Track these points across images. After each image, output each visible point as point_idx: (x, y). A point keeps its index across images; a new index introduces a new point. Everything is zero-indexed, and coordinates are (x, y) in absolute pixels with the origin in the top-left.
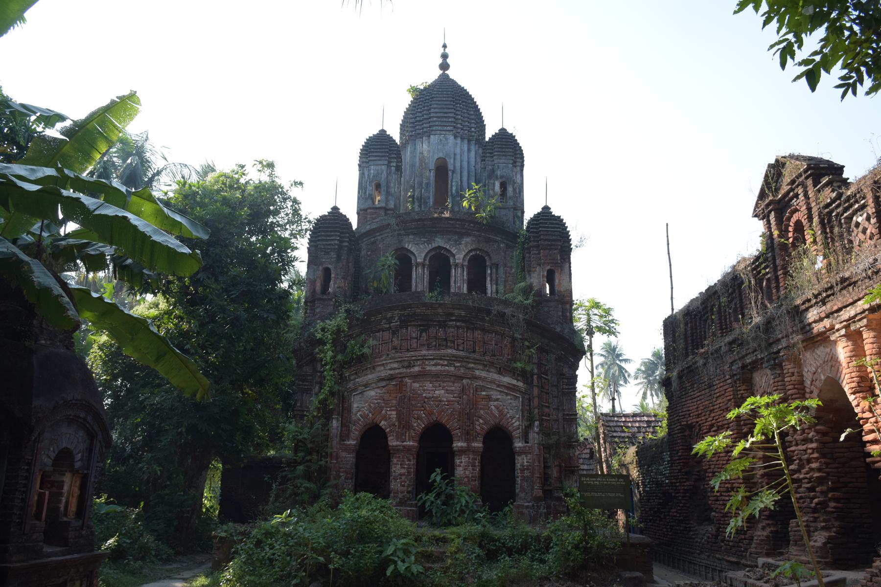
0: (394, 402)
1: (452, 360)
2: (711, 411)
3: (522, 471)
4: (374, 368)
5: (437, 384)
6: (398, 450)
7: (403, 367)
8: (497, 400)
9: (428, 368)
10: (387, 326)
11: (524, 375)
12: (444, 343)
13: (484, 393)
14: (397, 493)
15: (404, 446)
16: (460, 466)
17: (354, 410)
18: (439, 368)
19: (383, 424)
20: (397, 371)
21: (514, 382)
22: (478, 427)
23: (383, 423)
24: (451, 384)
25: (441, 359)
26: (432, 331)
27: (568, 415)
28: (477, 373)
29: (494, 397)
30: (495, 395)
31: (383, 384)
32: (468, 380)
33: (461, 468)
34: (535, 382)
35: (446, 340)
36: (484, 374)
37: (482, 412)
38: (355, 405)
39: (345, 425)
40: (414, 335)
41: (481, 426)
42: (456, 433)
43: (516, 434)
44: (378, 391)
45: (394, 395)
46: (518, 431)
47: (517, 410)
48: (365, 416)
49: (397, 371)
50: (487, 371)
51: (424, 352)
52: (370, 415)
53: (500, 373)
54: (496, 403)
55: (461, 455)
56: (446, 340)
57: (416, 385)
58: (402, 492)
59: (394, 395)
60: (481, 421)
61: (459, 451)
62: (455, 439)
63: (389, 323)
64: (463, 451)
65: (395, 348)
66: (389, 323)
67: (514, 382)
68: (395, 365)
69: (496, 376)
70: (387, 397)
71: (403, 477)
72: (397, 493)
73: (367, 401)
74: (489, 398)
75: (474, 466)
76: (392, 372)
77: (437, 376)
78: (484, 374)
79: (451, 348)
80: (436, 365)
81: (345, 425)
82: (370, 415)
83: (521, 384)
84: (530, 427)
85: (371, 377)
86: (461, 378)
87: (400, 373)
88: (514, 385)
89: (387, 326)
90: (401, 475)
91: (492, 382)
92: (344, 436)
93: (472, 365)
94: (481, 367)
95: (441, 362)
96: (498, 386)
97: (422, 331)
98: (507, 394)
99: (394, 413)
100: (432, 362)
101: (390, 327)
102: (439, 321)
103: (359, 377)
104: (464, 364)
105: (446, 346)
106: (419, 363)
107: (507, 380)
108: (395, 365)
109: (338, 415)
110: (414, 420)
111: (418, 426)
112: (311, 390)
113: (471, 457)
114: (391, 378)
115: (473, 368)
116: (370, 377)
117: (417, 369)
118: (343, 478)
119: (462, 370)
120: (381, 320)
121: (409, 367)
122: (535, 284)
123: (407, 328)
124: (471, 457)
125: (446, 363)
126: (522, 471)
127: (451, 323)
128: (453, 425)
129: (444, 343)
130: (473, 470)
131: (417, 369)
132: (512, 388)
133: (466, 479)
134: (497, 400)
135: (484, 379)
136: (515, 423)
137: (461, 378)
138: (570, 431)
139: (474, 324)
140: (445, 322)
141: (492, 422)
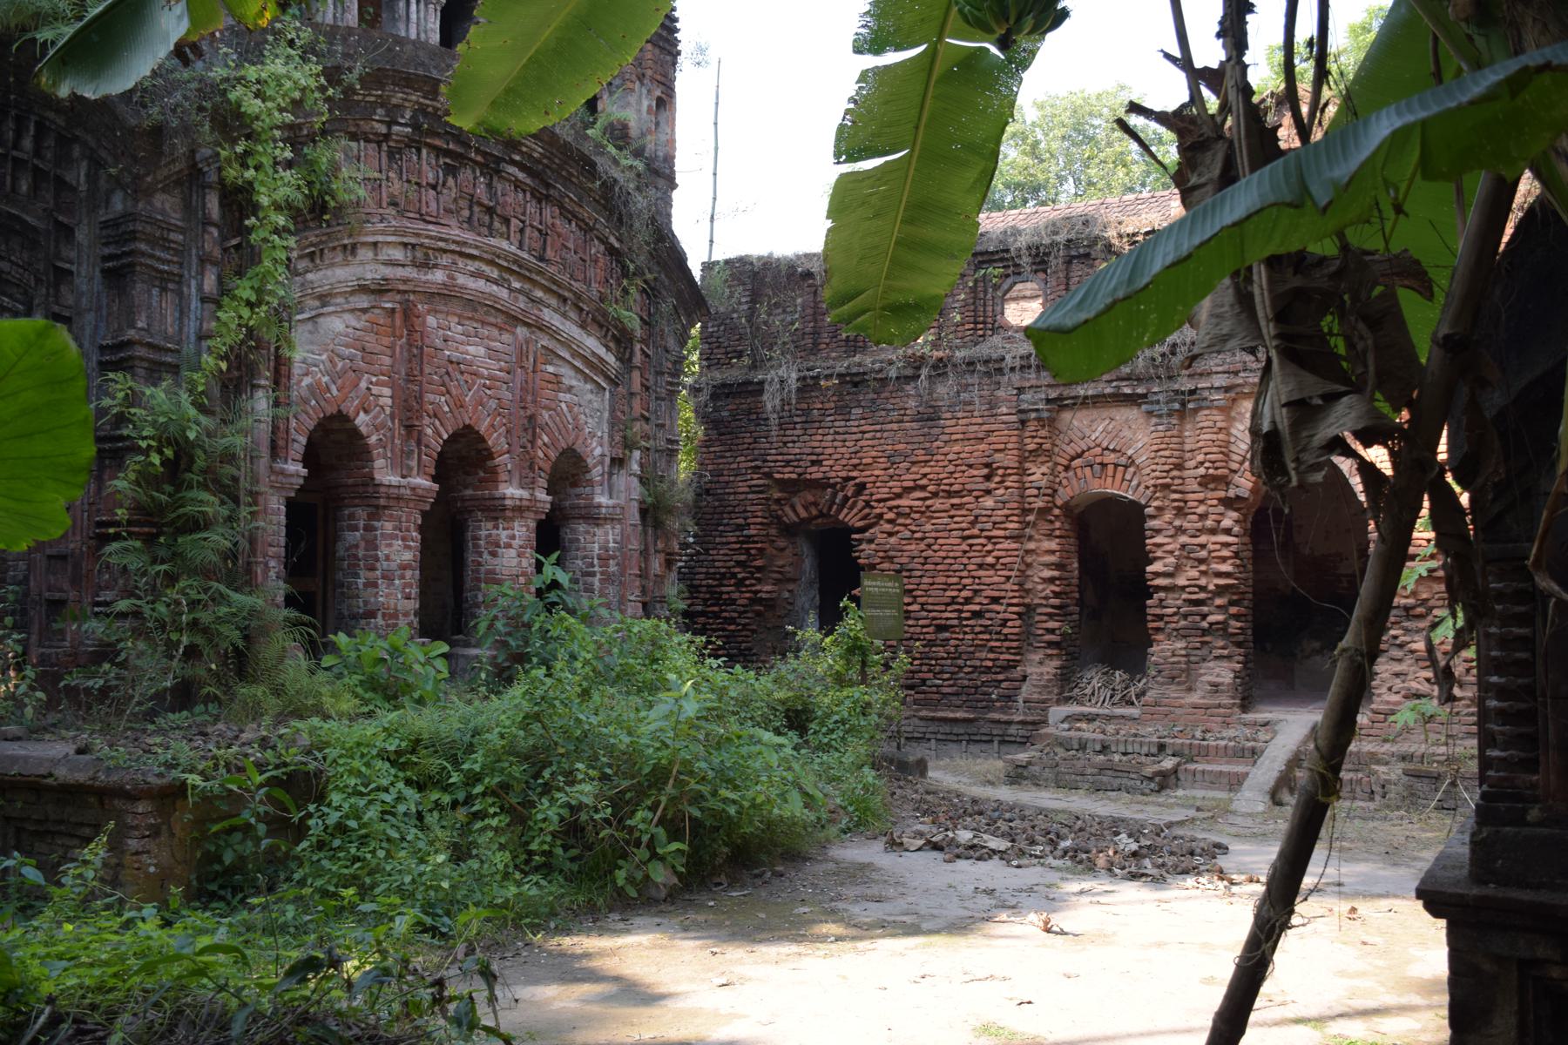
0: (387, 360)
1: (510, 269)
2: (913, 463)
3: (604, 560)
4: (354, 247)
5: (470, 326)
6: (398, 498)
7: (414, 264)
8: (570, 389)
9: (461, 280)
10: (383, 129)
11: (621, 340)
12: (491, 216)
13: (551, 369)
14: (395, 616)
15: (413, 489)
16: (509, 546)
17: (297, 370)
18: (481, 284)
19: (362, 420)
20: (400, 272)
21: (602, 351)
23: (362, 414)
24: (495, 332)
25: (491, 263)
26: (466, 174)
28: (548, 316)
29: (566, 381)
30: (570, 378)
31: (363, 301)
32: (525, 329)
33: (513, 552)
34: (638, 359)
35: (490, 211)
36: (555, 320)
38: (297, 356)
40: (431, 177)
43: (596, 473)
45: (386, 341)
47: (600, 418)
48: (317, 390)
49: (400, 272)
50: (564, 315)
51: (455, 232)
52: (335, 392)
53: (583, 326)
54: (568, 397)
55: (512, 519)
56: (490, 211)
57: (431, 321)
58: (406, 615)
59: (386, 341)
60: (546, 439)
61: (514, 509)
62: (503, 476)
63: (389, 124)
65: (394, 204)
66: (389, 124)
67: (602, 351)
68: (398, 254)
69: (575, 331)
70: (371, 342)
71: (408, 573)
72: (395, 616)
73: (328, 348)
74: (556, 380)
76: (389, 272)
77: (474, 307)
78: (555, 320)
79: (502, 235)
80: (477, 275)
82: (335, 392)
83: (611, 359)
86: (514, 320)
87: (405, 281)
88: (601, 359)
89: (383, 129)
90: (404, 567)
91: (566, 344)
93: (539, 294)
94: (554, 302)
95: (487, 269)
96: (575, 354)
97: (451, 171)
98: (587, 379)
100: (472, 266)
101: (387, 137)
102: (484, 154)
103: (317, 269)
104: (527, 286)
105: (490, 227)
106: (445, 260)
107: (592, 343)
108: (398, 254)
110: (426, 421)
111: (435, 434)
112: (180, 280)
114: (379, 290)
115: (540, 302)
117: (439, 276)
119: (522, 303)
120: (374, 106)
121: (425, 265)
122: (632, 124)
123: (419, 151)
125: (495, 274)
126: (604, 560)
127: (512, 169)
128: (496, 441)
129: (487, 218)
131: (439, 276)
132: (596, 365)
134: (570, 389)
135: (552, 332)
136: (597, 450)
137: (514, 320)
139: (548, 186)
140: (499, 160)
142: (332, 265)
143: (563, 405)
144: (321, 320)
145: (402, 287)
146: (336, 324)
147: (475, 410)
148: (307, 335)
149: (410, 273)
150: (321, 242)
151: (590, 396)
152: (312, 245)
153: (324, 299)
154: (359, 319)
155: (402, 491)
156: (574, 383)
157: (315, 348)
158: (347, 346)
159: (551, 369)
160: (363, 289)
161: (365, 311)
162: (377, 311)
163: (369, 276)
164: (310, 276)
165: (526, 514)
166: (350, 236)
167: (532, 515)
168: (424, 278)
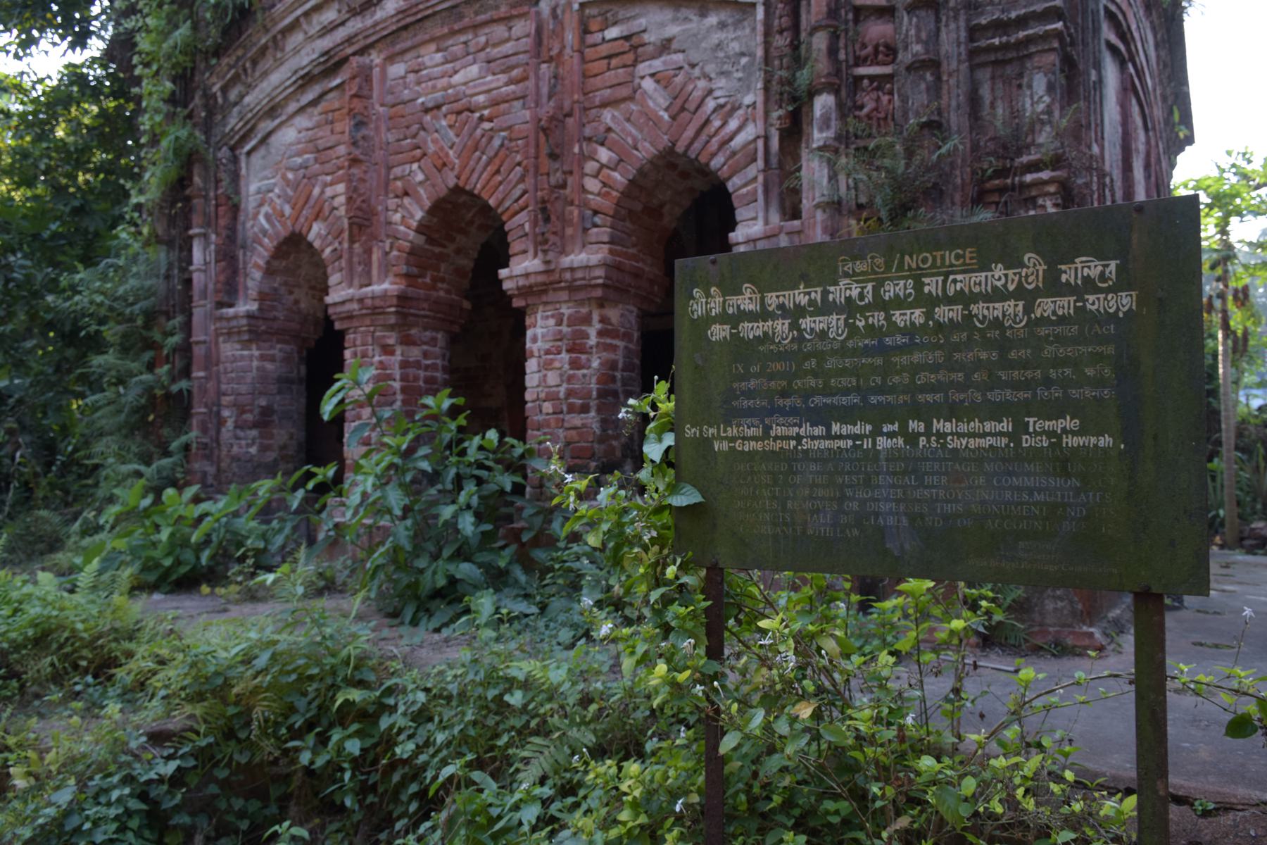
8: (665, 46)
13: (612, 33)
20: (341, 34)
22: (592, 185)
23: (316, 227)
24: (500, 31)
27: (1000, 26)
37: (608, 116)
38: (253, 188)
39: (229, 256)
41: (601, 176)
42: (520, 223)
44: (302, 121)
46: (752, 171)
49: (341, 34)
52: (287, 210)
54: (657, 64)
57: (397, 69)
64: (537, 291)
75: (577, 347)
76: (326, 43)
81: (229, 256)
84: (794, 131)
85: (277, 78)
87: (349, 40)
92: (229, 290)
99: (341, 188)
103: (250, 87)
109: (207, 224)
111: (406, 218)
113: (566, 310)
114: (332, 64)
116: (275, 78)
118: (230, 424)
124: (566, 310)
128: (509, 193)
130: (575, 364)
133: (548, 407)
134: (665, 46)
138: (1015, 113)
141: (647, 150)
142: (265, 74)
143: (648, 84)
144: (274, 139)
145: (349, 51)
146: (289, 135)
147: (463, 167)
148: (260, 162)
149: (355, 25)
150: (238, 59)
151: (716, 37)
152: (231, 67)
153: (272, 111)
154: (311, 116)
155: (348, 307)
156: (673, 30)
157: (267, 173)
158: (299, 154)
159: (612, 33)
160: (307, 80)
161: (314, 103)
162: (331, 95)
163: (305, 62)
164: (247, 99)
165: (551, 296)
166: (267, 31)
167: (564, 295)
168: (369, 22)
